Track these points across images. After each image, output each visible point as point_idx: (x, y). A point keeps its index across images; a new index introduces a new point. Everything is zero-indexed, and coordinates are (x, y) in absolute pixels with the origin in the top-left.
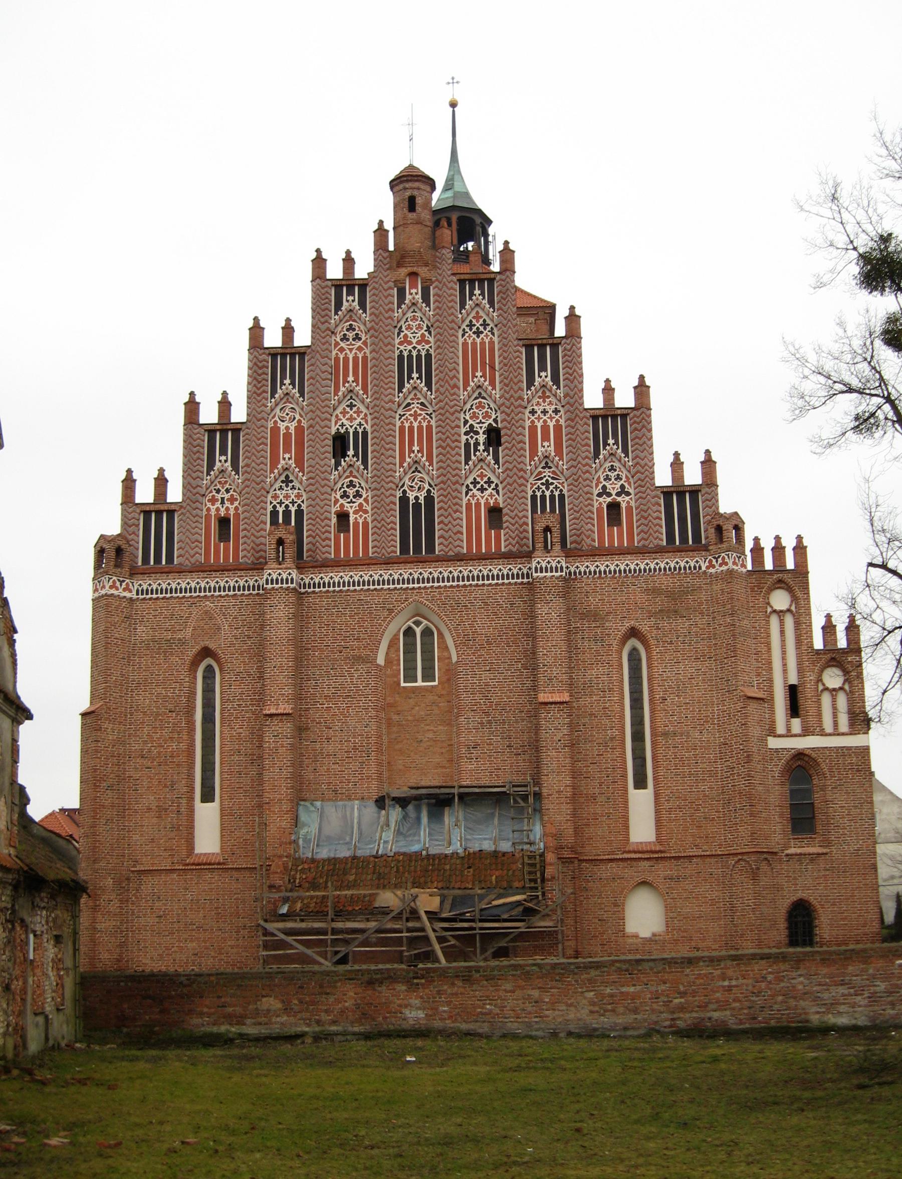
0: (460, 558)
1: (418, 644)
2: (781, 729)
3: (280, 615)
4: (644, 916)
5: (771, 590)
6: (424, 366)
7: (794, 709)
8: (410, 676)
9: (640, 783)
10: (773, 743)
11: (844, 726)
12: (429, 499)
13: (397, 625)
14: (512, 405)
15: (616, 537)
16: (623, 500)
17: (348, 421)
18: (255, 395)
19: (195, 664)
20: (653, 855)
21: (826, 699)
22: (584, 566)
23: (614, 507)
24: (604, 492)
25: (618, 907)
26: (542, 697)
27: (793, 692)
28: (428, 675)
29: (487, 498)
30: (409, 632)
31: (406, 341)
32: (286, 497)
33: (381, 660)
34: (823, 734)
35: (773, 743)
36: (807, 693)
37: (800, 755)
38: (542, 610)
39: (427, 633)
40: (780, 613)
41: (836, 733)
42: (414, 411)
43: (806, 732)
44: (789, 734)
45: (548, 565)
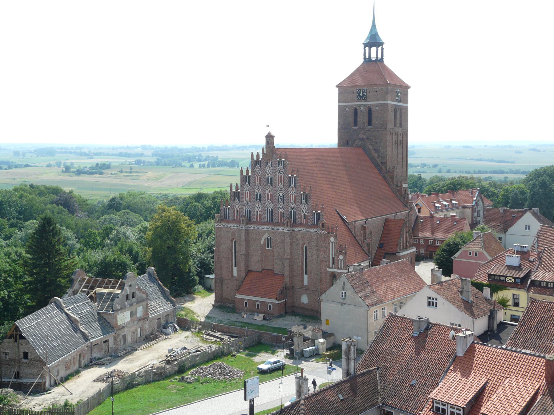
1: (269, 241)
2: (331, 266)
4: (305, 299)
5: (330, 237)
6: (270, 181)
7: (333, 263)
8: (268, 247)
9: (306, 273)
10: (328, 270)
11: (342, 268)
12: (272, 210)
13: (265, 236)
15: (305, 222)
16: (306, 213)
17: (258, 192)
19: (232, 241)
20: (306, 288)
21: (340, 261)
22: (296, 229)
23: (305, 214)
24: (303, 212)
25: (300, 297)
26: (285, 257)
27: (333, 259)
28: (271, 247)
29: (282, 211)
30: (267, 238)
31: (268, 174)
32: (247, 207)
33: (262, 243)
34: (338, 268)
35: (328, 270)
36: (336, 259)
37: (333, 272)
38: (286, 239)
39: (270, 238)
40: (332, 243)
41: (341, 269)
42: (269, 191)
43: (335, 268)
44: (332, 268)
45: (288, 230)
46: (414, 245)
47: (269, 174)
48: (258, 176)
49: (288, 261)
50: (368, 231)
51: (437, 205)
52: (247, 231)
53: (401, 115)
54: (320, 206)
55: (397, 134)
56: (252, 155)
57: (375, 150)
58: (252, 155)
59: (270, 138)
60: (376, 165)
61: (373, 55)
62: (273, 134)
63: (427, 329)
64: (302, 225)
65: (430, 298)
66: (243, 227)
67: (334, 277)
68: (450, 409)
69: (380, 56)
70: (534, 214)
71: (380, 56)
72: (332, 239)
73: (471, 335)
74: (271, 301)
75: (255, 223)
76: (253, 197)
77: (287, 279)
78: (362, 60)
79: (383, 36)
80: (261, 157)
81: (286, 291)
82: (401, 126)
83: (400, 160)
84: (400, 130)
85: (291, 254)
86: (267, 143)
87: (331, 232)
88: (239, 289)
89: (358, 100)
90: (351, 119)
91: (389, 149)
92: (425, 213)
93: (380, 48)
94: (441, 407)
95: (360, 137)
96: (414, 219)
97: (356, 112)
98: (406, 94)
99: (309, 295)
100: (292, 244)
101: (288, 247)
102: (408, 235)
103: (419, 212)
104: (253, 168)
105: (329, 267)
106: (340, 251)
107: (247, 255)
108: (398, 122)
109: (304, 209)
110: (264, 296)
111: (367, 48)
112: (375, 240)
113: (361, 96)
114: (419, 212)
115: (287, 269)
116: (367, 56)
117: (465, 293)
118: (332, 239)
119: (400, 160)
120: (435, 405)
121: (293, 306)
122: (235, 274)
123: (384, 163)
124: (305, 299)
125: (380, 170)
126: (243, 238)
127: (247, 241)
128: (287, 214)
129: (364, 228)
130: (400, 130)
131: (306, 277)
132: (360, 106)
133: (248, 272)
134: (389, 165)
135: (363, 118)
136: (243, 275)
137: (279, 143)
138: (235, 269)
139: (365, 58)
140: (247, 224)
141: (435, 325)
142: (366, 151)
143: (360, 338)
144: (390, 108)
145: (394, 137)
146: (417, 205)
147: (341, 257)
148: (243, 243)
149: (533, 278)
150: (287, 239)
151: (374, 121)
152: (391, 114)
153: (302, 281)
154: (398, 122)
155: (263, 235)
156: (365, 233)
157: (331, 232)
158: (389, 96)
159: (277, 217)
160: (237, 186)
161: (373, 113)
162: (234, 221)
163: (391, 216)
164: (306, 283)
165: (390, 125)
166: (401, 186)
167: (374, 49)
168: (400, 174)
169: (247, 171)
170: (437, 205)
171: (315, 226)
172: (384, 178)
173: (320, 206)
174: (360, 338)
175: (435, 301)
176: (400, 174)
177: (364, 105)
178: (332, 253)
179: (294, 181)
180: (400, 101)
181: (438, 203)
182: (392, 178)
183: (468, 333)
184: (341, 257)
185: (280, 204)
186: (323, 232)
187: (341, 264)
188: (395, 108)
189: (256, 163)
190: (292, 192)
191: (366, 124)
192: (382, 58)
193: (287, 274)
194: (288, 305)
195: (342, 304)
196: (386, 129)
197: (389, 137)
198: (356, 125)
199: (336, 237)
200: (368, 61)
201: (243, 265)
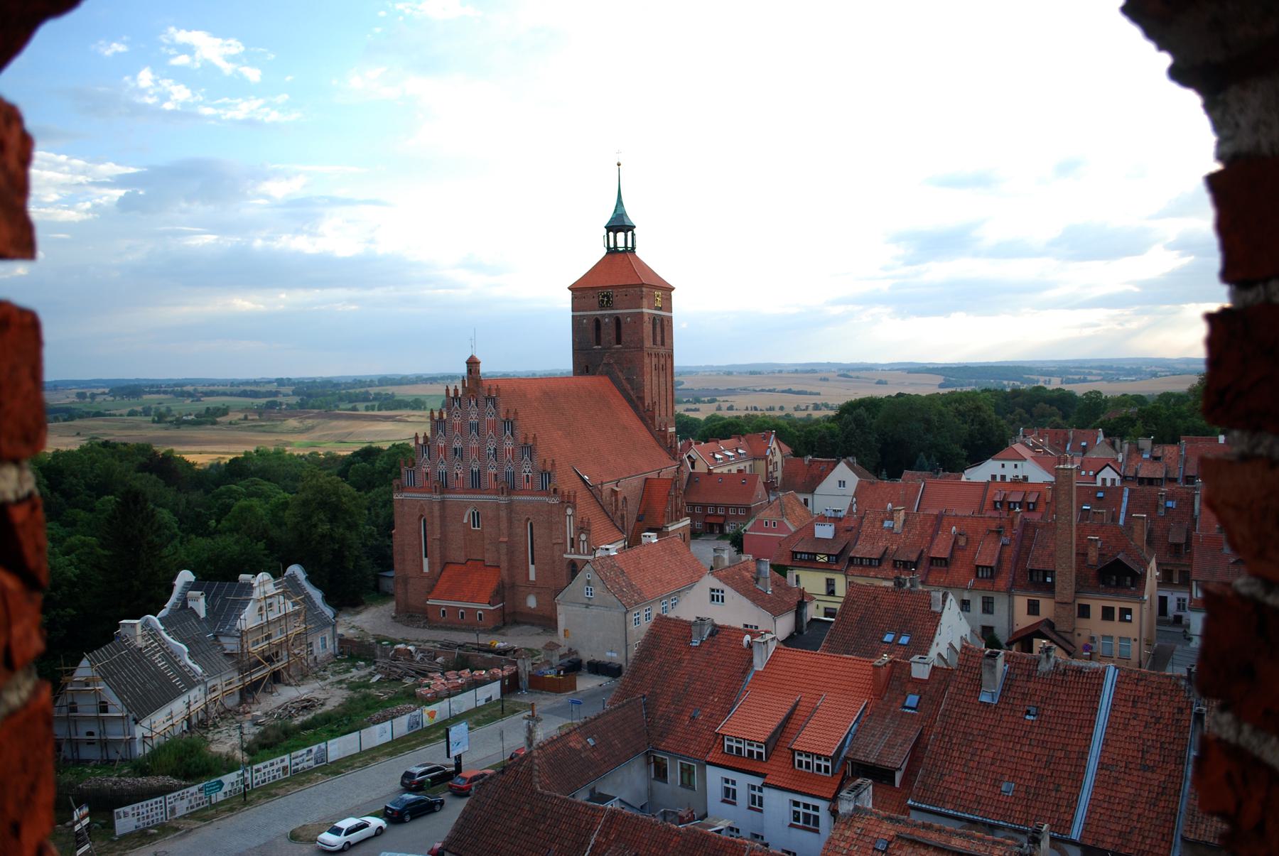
0: (487, 491)
1: (476, 517)
3: (436, 508)
4: (532, 602)
6: (476, 427)
7: (572, 546)
13: (470, 511)
14: (500, 442)
18: (432, 434)
20: (534, 585)
22: (515, 498)
25: (525, 599)
27: (572, 540)
29: (494, 471)
32: (442, 468)
45: (503, 499)
46: (687, 515)
47: (473, 418)
48: (457, 421)
49: (504, 546)
50: (620, 498)
51: (718, 456)
52: (443, 502)
53: (663, 327)
54: (549, 462)
55: (657, 355)
56: (447, 390)
57: (627, 379)
58: (447, 390)
59: (473, 364)
60: (630, 401)
61: (621, 244)
62: (479, 357)
63: (711, 635)
64: (524, 492)
65: (713, 590)
66: (437, 497)
67: (574, 568)
68: (747, 747)
69: (630, 245)
70: (849, 465)
71: (630, 245)
72: (569, 511)
73: (773, 639)
74: (481, 607)
75: (453, 491)
76: (450, 453)
77: (504, 573)
78: (603, 252)
79: (633, 216)
80: (460, 392)
81: (505, 592)
82: (663, 344)
83: (663, 393)
84: (662, 351)
85: (510, 535)
86: (469, 371)
87: (568, 501)
88: (431, 590)
89: (602, 307)
90: (591, 335)
91: (647, 378)
92: (701, 468)
93: (630, 233)
94: (735, 745)
95: (605, 361)
96: (685, 476)
97: (597, 322)
98: (668, 299)
99: (538, 595)
100: (510, 521)
101: (504, 525)
102: (679, 501)
103: (693, 467)
104: (449, 409)
105: (565, 552)
106: (583, 528)
107: (444, 539)
108: (659, 338)
109: (526, 469)
110: (472, 600)
111: (611, 234)
112: (632, 509)
113: (606, 300)
114: (693, 467)
115: (504, 558)
116: (612, 245)
117: (761, 580)
118: (569, 511)
119: (663, 393)
120: (726, 743)
121: (514, 613)
122: (426, 569)
123: (642, 399)
124: (532, 602)
125: (635, 408)
126: (437, 512)
127: (443, 518)
128: (502, 477)
129: (614, 492)
130: (662, 351)
131: (532, 568)
132: (603, 316)
133: (445, 565)
134: (648, 401)
135: (608, 334)
136: (438, 569)
137: (484, 369)
138: (425, 561)
139: (608, 248)
140: (442, 493)
141: (722, 627)
142: (615, 381)
143: (615, 655)
144: (646, 318)
145: (654, 360)
146: (689, 457)
147: (583, 537)
148: (437, 522)
149: (852, 554)
150: (503, 514)
151: (624, 338)
152: (648, 327)
153: (527, 575)
154: (659, 338)
155: (467, 507)
156: (616, 500)
157: (568, 501)
158: (645, 302)
159: (488, 482)
160: (425, 437)
161: (623, 325)
162: (422, 490)
163: (653, 475)
164: (532, 577)
165: (648, 343)
166: (666, 431)
167: (621, 236)
168: (663, 413)
169: (441, 413)
170: (718, 456)
171: (544, 491)
172: (642, 419)
173: (549, 462)
174: (615, 655)
175: (720, 594)
176: (663, 413)
177: (610, 315)
178: (570, 532)
179: (509, 424)
180: (660, 309)
181: (719, 453)
182: (653, 419)
183: (768, 636)
184: (583, 537)
185: (492, 462)
186: (554, 501)
187: (583, 547)
188: (654, 319)
189: (452, 401)
190: (509, 445)
191: (614, 341)
192: (633, 248)
193: (504, 565)
194: (507, 611)
195: (587, 606)
196: (642, 348)
197: (647, 360)
198: (598, 344)
199: (574, 508)
200: (612, 251)
201: (437, 555)
